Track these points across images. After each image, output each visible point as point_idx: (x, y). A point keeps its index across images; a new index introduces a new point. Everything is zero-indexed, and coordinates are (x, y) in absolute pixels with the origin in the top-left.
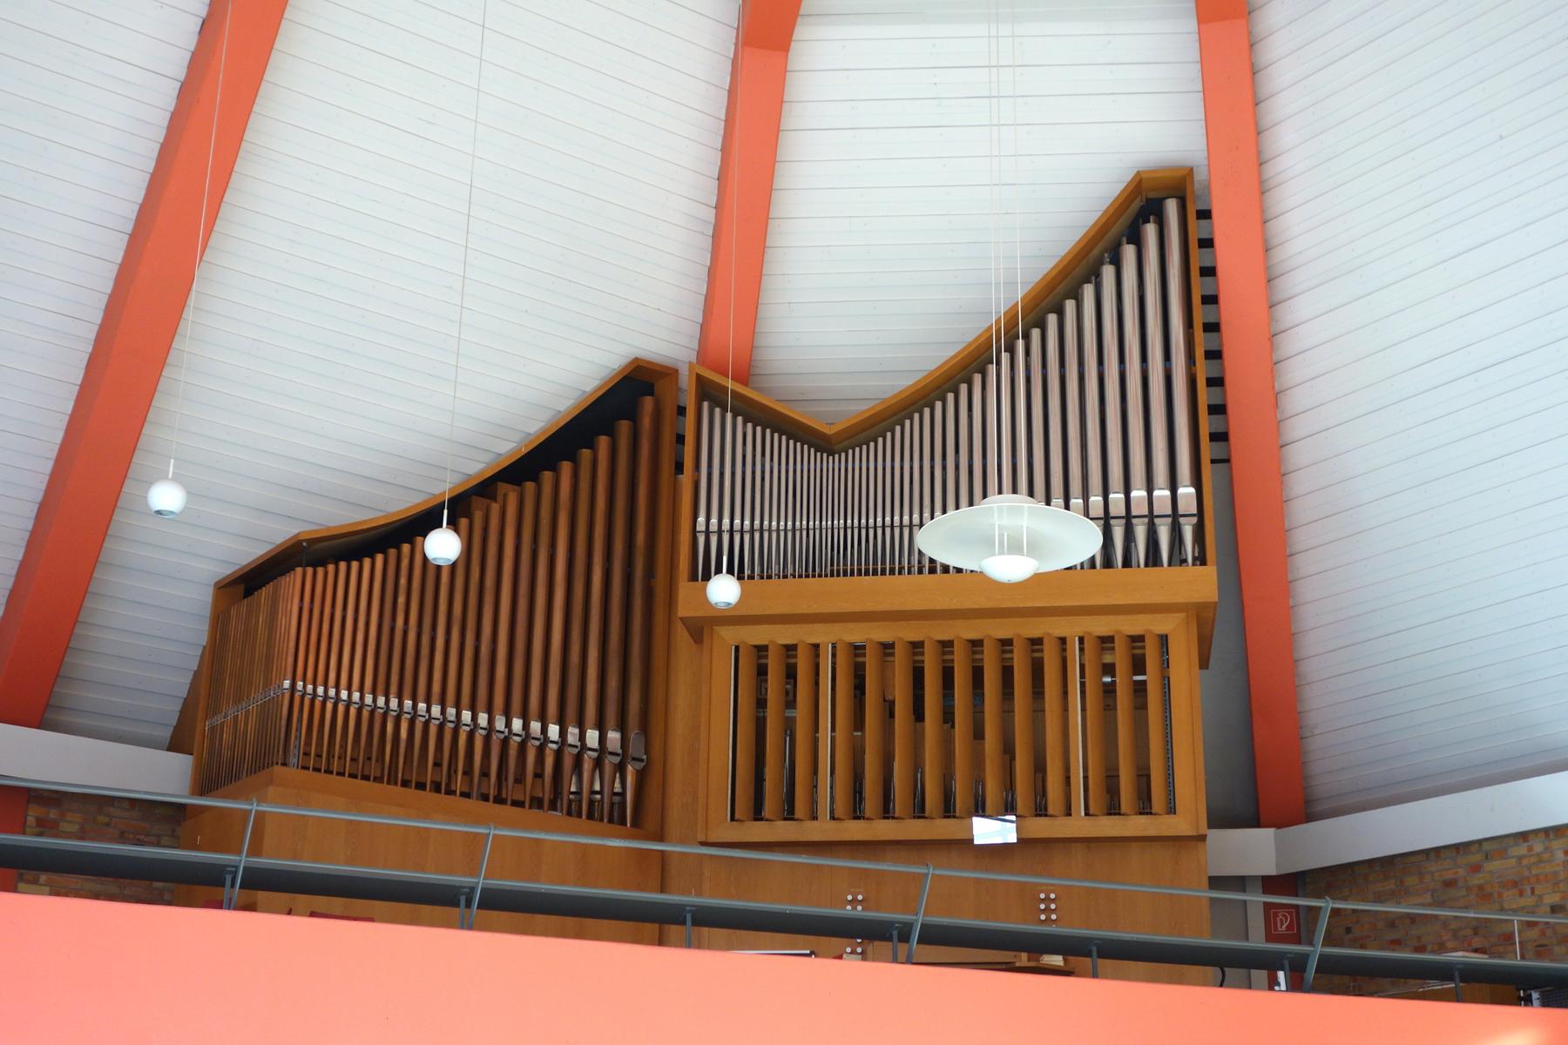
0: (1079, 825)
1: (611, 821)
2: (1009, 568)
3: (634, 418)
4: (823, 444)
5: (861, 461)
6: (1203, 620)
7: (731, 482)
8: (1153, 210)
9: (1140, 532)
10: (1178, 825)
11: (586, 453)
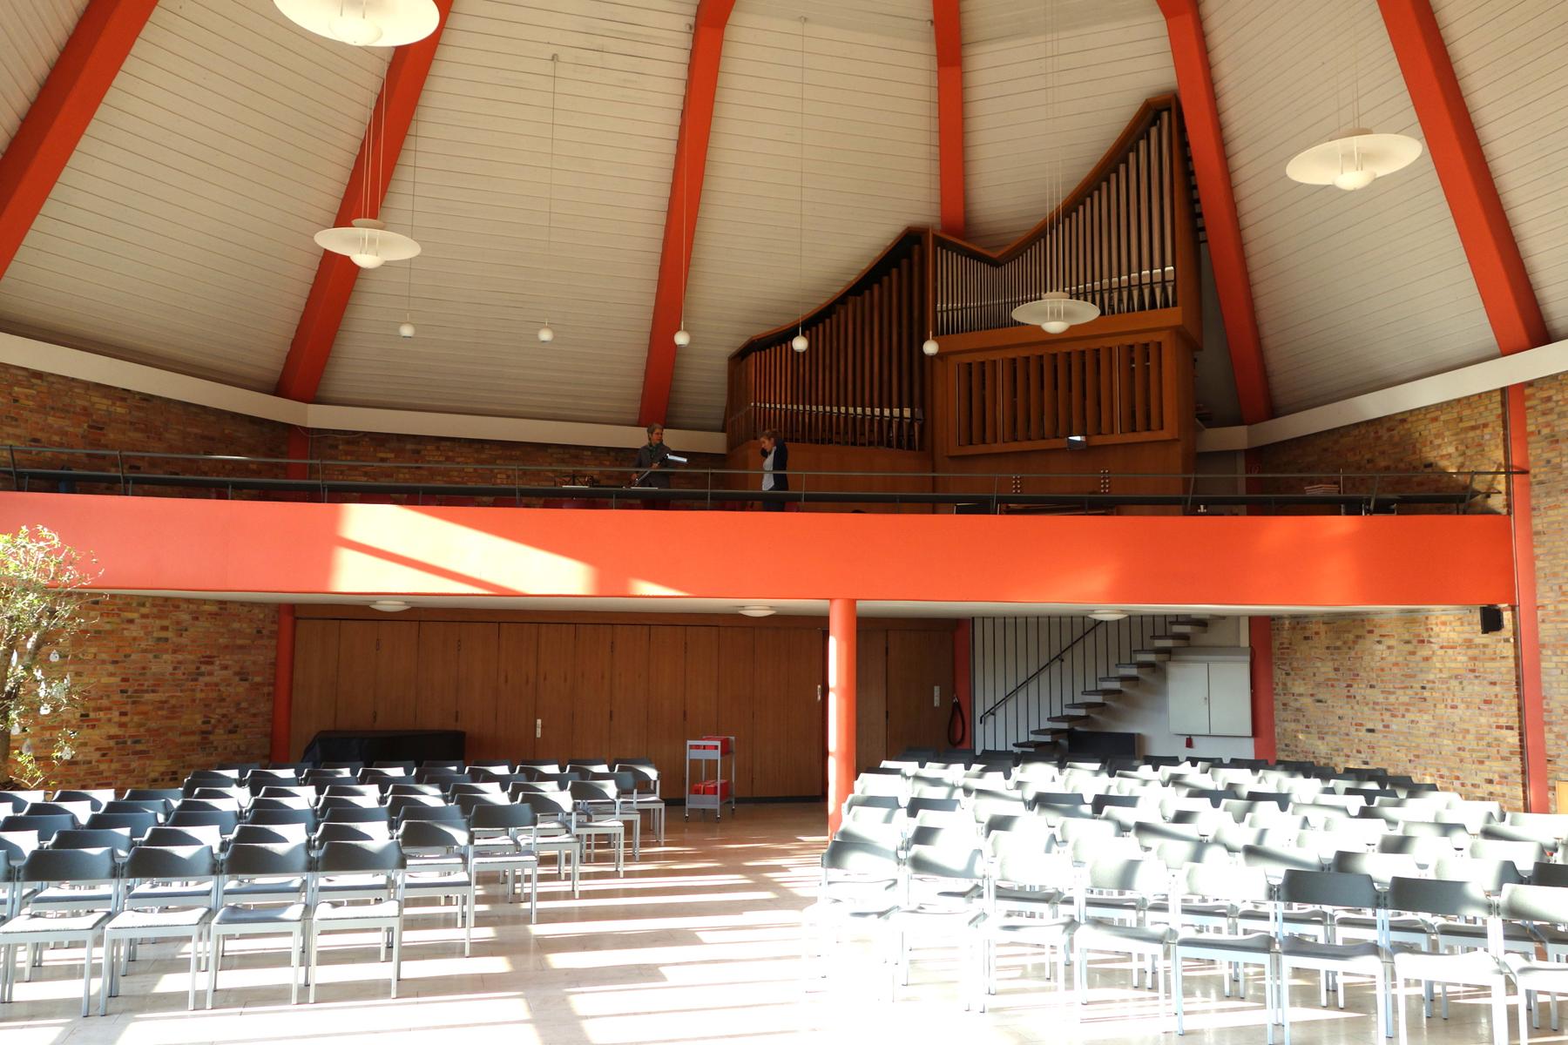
0: (1118, 438)
1: (900, 446)
2: (1055, 327)
3: (910, 257)
4: (995, 263)
5: (1011, 269)
6: (1178, 332)
7: (954, 289)
8: (1159, 114)
9: (1135, 293)
10: (1164, 435)
11: (886, 278)
